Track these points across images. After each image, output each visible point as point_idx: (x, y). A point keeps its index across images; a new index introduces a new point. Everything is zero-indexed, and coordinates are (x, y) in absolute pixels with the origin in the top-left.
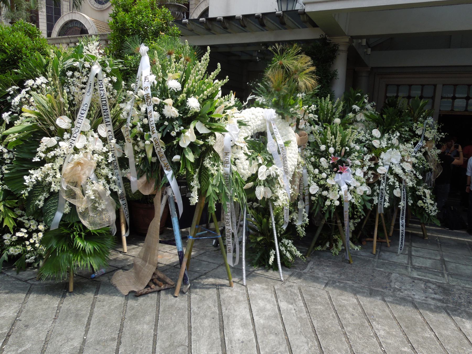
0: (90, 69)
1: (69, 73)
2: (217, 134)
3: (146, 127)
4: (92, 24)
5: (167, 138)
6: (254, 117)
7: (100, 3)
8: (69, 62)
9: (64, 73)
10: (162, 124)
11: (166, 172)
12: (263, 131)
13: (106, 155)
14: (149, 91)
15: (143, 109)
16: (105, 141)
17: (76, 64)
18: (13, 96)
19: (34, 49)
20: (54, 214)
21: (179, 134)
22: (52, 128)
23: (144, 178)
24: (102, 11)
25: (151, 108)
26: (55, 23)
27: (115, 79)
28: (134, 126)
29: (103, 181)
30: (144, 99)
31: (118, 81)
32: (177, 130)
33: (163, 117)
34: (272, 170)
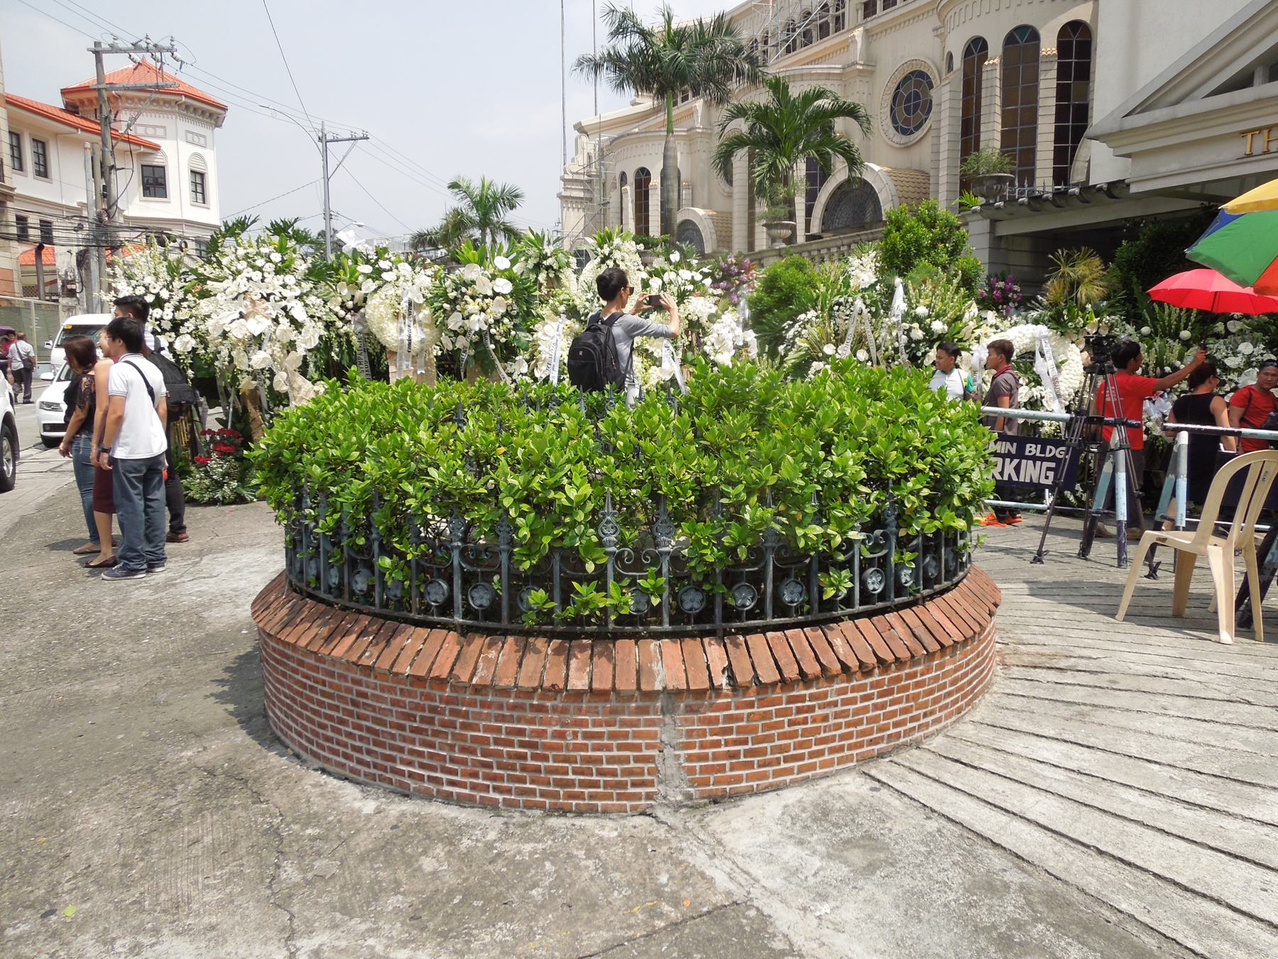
1: (836, 308)
2: (963, 353)
3: (896, 350)
4: (885, 179)
7: (905, 132)
8: (836, 298)
9: (831, 309)
15: (894, 334)
17: (842, 300)
18: (787, 331)
19: (805, 284)
21: (925, 354)
24: (907, 147)
25: (900, 333)
26: (821, 185)
28: (887, 350)
30: (894, 325)
33: (910, 340)
34: (1036, 392)
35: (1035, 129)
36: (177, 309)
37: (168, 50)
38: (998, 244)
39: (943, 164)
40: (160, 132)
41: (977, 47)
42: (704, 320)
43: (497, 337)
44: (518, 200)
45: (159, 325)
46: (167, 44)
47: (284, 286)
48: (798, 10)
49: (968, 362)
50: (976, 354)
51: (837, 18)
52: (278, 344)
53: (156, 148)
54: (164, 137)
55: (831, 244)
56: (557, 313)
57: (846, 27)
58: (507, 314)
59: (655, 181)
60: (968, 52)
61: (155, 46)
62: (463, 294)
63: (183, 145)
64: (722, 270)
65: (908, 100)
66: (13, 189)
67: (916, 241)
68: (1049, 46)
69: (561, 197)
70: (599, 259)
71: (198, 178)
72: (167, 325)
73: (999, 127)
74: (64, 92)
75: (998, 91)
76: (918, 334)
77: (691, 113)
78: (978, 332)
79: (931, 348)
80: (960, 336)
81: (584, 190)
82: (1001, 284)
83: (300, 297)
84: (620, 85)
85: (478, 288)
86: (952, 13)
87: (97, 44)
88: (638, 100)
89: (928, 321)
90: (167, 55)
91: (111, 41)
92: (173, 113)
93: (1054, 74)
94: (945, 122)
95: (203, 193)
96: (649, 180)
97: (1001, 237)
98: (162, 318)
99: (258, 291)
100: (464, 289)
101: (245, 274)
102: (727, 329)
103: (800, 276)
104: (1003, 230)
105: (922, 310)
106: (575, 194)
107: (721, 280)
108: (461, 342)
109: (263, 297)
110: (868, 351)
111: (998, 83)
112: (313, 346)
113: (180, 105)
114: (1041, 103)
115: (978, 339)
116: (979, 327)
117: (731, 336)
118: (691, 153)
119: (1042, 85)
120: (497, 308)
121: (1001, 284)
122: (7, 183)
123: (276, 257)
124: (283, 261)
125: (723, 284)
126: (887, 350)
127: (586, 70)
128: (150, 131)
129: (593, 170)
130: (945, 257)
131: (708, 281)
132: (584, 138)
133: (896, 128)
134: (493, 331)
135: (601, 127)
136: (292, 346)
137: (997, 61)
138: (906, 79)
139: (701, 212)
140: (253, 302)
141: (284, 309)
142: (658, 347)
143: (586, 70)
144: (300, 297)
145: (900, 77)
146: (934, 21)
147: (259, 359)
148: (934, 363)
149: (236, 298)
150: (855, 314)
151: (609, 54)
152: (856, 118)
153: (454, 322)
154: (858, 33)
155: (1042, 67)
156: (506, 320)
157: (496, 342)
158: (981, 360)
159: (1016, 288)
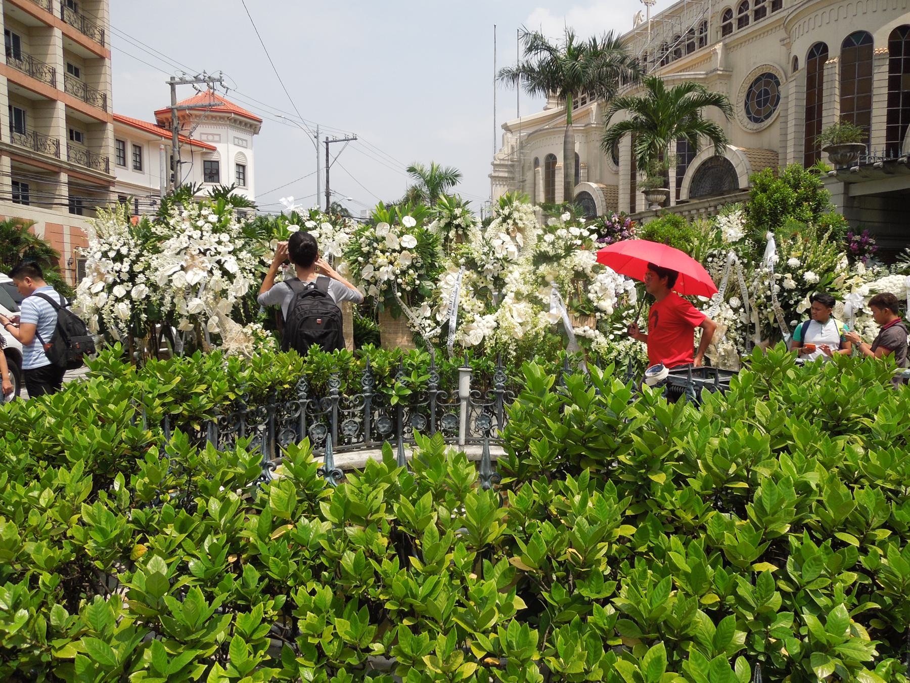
0: (725, 256)
1: (710, 259)
3: (769, 298)
5: (786, 306)
6: (892, 285)
7: (757, 120)
8: (711, 251)
9: (705, 260)
10: (782, 295)
11: (784, 334)
12: (904, 299)
13: (735, 321)
14: (772, 269)
15: (766, 283)
16: (736, 310)
17: (715, 252)
19: (680, 239)
21: (797, 302)
22: (695, 301)
23: (767, 341)
24: (759, 132)
25: (773, 283)
26: (689, 163)
27: (746, 261)
28: (759, 298)
29: (731, 342)
30: (767, 275)
31: (749, 262)
32: (796, 299)
33: (783, 289)
35: (869, 113)
36: (134, 262)
37: (218, 80)
38: (851, 203)
39: (790, 143)
40: (217, 138)
41: (819, 51)
42: (588, 271)
43: (403, 286)
44: (458, 179)
45: (119, 277)
46: (217, 76)
47: (219, 243)
48: (671, 35)
49: (841, 310)
50: (847, 302)
51: (701, 39)
52: (211, 293)
53: (214, 149)
54: (219, 142)
55: (700, 206)
56: (458, 265)
57: (709, 44)
58: (412, 266)
59: (560, 163)
60: (811, 55)
61: (209, 77)
62: (375, 249)
63: (231, 146)
64: (607, 227)
65: (759, 96)
66: (115, 178)
67: (782, 200)
68: (881, 46)
69: (491, 177)
70: (500, 219)
71: (241, 169)
72: (125, 277)
73: (838, 113)
74: (157, 113)
75: (837, 84)
76: (790, 283)
77: (588, 113)
78: (849, 282)
79: (804, 297)
80: (831, 286)
81: (508, 172)
82: (857, 238)
83: (233, 252)
84: (533, 90)
85: (388, 244)
86: (797, 26)
87: (173, 78)
88: (549, 106)
89: (800, 271)
90: (217, 84)
91: (181, 76)
92: (224, 125)
93: (886, 68)
94: (792, 110)
95: (244, 179)
96: (556, 163)
97: (854, 197)
99: (197, 247)
100: (375, 245)
101: (187, 233)
102: (610, 279)
103: (676, 232)
104: (856, 191)
105: (793, 262)
106: (501, 174)
107: (606, 236)
108: (373, 290)
109: (200, 252)
110: (741, 298)
111: (837, 77)
112: (244, 293)
113: (230, 120)
114: (875, 92)
115: (849, 288)
116: (851, 277)
117: (613, 285)
118: (587, 142)
119: (876, 77)
120: (404, 261)
121: (857, 238)
122: (111, 174)
123: (214, 218)
124: (219, 221)
125: (608, 239)
126: (759, 298)
127: (505, 79)
128: (210, 138)
129: (515, 157)
130: (809, 214)
131: (594, 237)
132: (509, 135)
133: (750, 118)
134: (399, 281)
135: (521, 126)
136: (224, 293)
137: (836, 60)
138: (758, 80)
139: (594, 185)
140: (192, 256)
141: (219, 262)
142: (547, 294)
143: (505, 79)
144: (233, 252)
145: (753, 78)
146: (782, 34)
147: (195, 305)
148: (808, 311)
149: (178, 253)
150: (729, 264)
151: (523, 66)
152: (720, 106)
153: (367, 273)
154: (719, 47)
155: (875, 63)
156: (411, 271)
157: (403, 291)
158: (853, 308)
159: (872, 241)
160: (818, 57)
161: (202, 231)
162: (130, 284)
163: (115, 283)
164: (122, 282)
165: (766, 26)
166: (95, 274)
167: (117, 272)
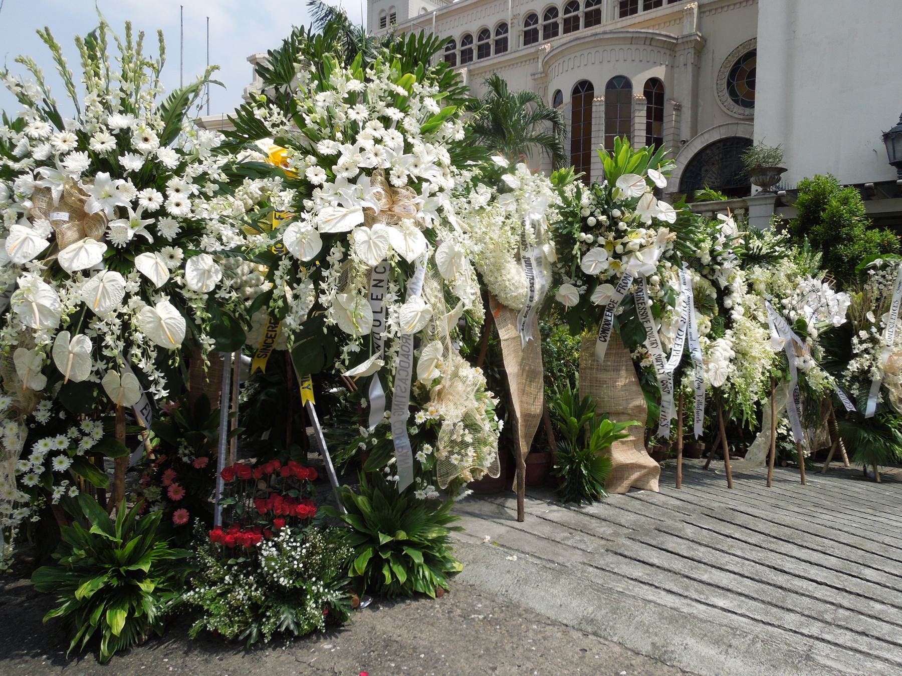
20: (866, 404)
41: (584, 89)
60: (576, 91)
62: (614, 221)
68: (638, 92)
72: (168, 229)
75: (603, 121)
86: (556, 64)
93: (644, 113)
98: (162, 212)
100: (616, 213)
101: (369, 130)
108: (601, 295)
109: (411, 182)
119: (637, 120)
137: (603, 98)
149: (353, 181)
155: (635, 107)
160: (583, 93)
161: (404, 132)
162: (179, 252)
163: (138, 245)
164: (159, 244)
165: (507, 60)
166: (64, 216)
167: (146, 215)
